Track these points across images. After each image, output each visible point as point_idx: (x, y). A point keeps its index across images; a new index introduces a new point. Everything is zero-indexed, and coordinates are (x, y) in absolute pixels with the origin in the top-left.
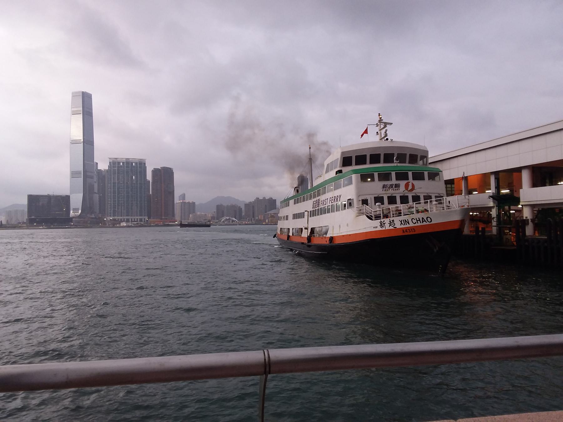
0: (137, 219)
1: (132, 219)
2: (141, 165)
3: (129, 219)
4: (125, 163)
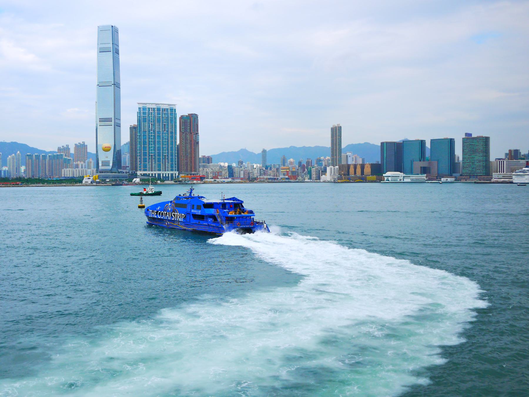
0: (168, 174)
1: (163, 174)
2: (173, 111)
3: (160, 174)
4: (156, 109)
